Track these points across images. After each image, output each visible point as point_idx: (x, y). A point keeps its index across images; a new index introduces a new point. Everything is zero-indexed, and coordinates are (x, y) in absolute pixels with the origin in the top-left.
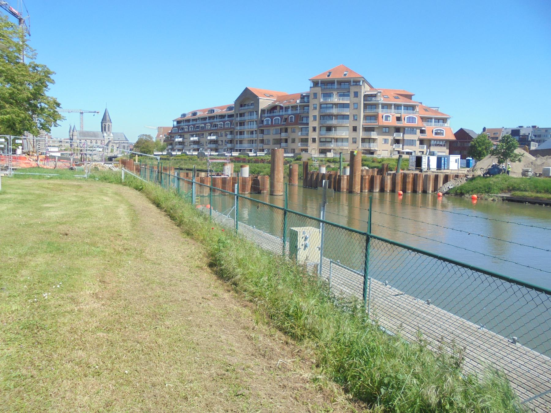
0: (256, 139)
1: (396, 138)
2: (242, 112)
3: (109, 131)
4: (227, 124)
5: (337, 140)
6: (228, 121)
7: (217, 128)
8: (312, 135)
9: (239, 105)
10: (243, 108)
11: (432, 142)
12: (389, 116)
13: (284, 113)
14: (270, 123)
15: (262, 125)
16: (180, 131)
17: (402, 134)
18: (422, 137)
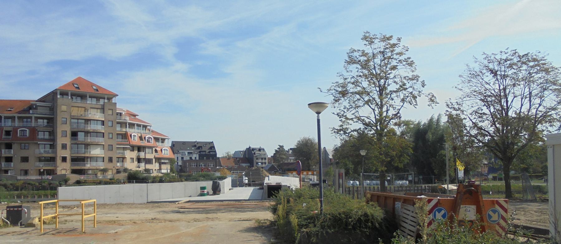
5: (92, 158)
8: (61, 153)
18: (157, 156)
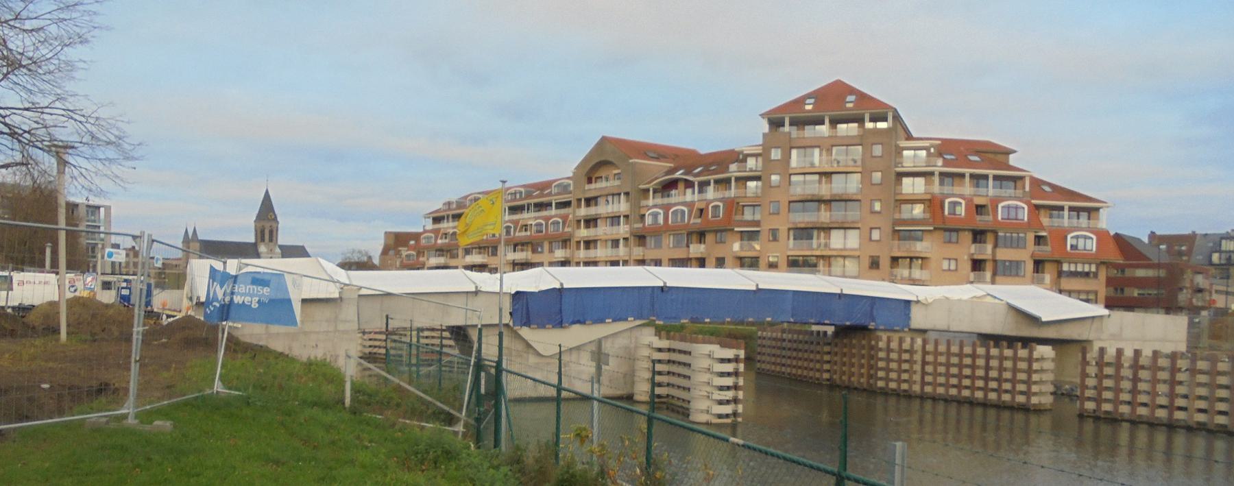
0: (626, 258)
1: (976, 257)
2: (589, 195)
3: (271, 240)
4: (553, 223)
6: (556, 216)
7: (528, 233)
9: (585, 179)
10: (593, 186)
11: (1065, 267)
12: (960, 203)
13: (696, 197)
14: (661, 220)
15: (640, 225)
16: (439, 241)
17: (989, 247)
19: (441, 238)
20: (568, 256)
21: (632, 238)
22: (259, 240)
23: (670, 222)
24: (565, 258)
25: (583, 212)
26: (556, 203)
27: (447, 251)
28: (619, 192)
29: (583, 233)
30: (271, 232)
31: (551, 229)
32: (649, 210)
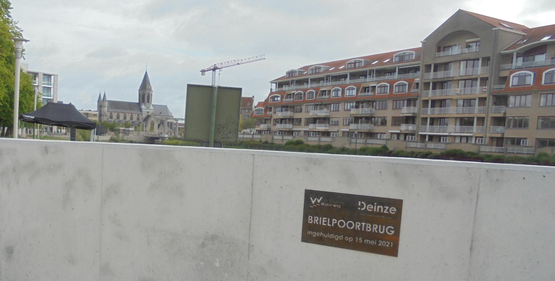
0: (483, 115)
2: (438, 61)
3: (148, 102)
4: (399, 85)
10: (442, 54)
14: (530, 81)
19: (287, 98)
20: (416, 112)
21: (491, 97)
22: (141, 101)
23: (543, 83)
24: (413, 113)
25: (431, 75)
26: (399, 69)
27: (291, 107)
28: (477, 57)
29: (431, 94)
30: (148, 97)
31: (396, 90)
32: (511, 73)
